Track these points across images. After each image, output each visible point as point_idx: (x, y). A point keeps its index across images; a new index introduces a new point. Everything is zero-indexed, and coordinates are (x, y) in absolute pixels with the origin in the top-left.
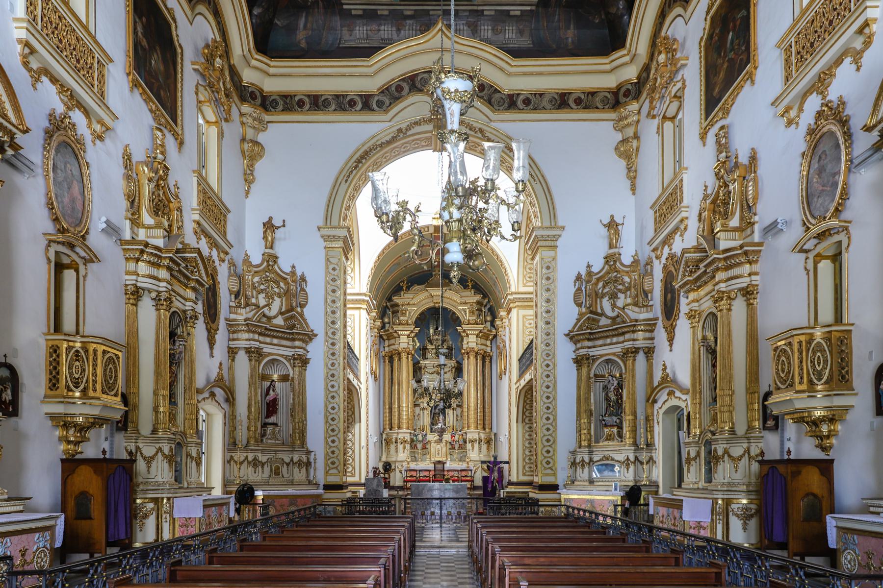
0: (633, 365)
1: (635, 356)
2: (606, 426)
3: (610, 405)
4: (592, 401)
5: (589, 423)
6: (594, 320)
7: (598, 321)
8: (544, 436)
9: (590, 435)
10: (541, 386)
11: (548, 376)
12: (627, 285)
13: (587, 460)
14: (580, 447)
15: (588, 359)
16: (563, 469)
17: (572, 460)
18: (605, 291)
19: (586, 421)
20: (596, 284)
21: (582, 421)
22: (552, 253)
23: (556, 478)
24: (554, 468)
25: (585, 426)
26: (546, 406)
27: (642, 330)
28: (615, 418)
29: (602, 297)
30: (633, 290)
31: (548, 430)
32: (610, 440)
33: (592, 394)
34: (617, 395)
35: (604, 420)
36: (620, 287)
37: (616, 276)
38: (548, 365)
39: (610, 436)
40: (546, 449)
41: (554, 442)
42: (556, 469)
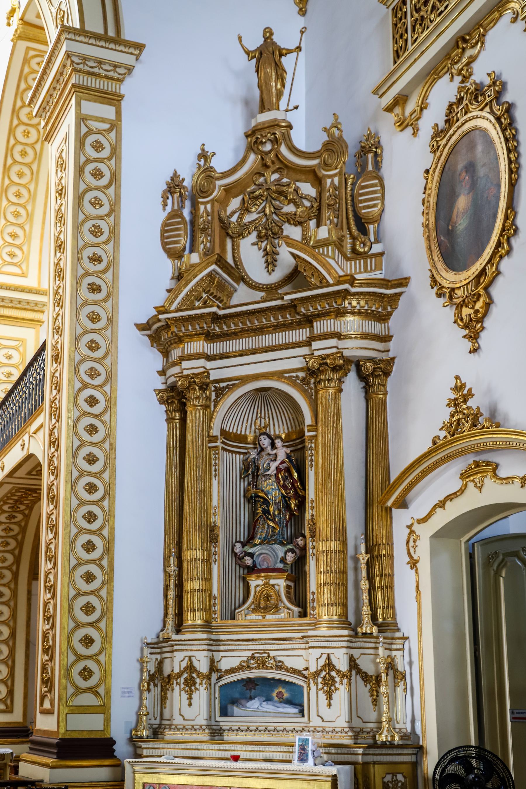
0: (337, 401)
1: (340, 381)
2: (253, 570)
3: (266, 512)
4: (215, 502)
5: (208, 562)
6: (222, 286)
7: (230, 296)
8: (79, 594)
9: (210, 596)
10: (75, 455)
11: (92, 429)
12: (307, 204)
13: (203, 667)
14: (179, 628)
15: (204, 387)
16: (126, 692)
17: (152, 667)
18: (248, 218)
19: (199, 554)
20: (224, 202)
21: (188, 555)
22: (108, 112)
23: (107, 721)
24: (101, 690)
25: (198, 570)
26: (84, 510)
27: (360, 313)
28: (280, 551)
29: (241, 235)
30: (327, 214)
31: (89, 577)
32: (266, 609)
33: (215, 483)
34: (284, 487)
35: (251, 555)
36: (290, 209)
37: (278, 182)
38: (92, 401)
39: (268, 598)
40: (81, 633)
41: (107, 612)
42: (108, 692)
